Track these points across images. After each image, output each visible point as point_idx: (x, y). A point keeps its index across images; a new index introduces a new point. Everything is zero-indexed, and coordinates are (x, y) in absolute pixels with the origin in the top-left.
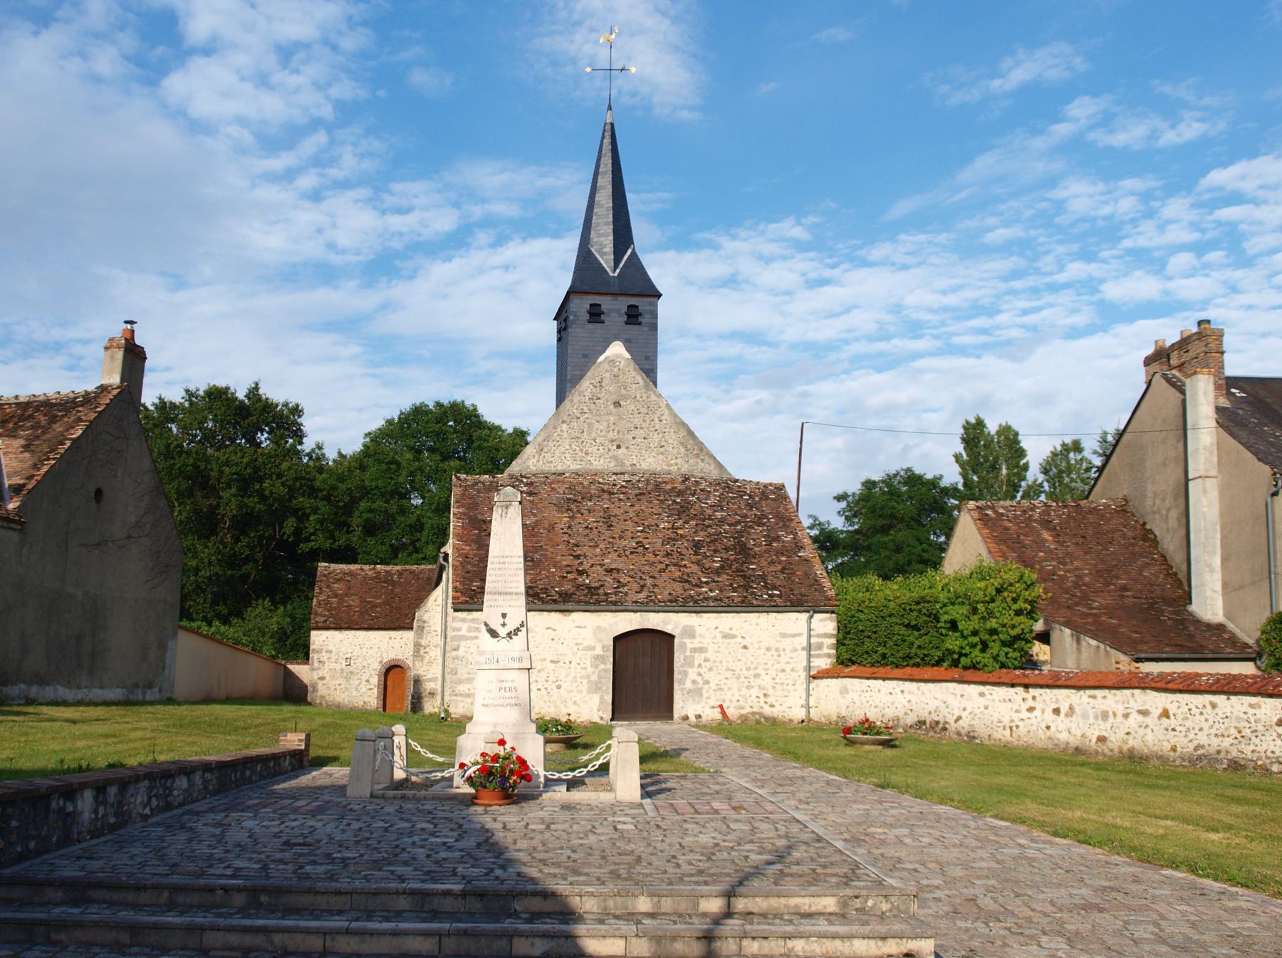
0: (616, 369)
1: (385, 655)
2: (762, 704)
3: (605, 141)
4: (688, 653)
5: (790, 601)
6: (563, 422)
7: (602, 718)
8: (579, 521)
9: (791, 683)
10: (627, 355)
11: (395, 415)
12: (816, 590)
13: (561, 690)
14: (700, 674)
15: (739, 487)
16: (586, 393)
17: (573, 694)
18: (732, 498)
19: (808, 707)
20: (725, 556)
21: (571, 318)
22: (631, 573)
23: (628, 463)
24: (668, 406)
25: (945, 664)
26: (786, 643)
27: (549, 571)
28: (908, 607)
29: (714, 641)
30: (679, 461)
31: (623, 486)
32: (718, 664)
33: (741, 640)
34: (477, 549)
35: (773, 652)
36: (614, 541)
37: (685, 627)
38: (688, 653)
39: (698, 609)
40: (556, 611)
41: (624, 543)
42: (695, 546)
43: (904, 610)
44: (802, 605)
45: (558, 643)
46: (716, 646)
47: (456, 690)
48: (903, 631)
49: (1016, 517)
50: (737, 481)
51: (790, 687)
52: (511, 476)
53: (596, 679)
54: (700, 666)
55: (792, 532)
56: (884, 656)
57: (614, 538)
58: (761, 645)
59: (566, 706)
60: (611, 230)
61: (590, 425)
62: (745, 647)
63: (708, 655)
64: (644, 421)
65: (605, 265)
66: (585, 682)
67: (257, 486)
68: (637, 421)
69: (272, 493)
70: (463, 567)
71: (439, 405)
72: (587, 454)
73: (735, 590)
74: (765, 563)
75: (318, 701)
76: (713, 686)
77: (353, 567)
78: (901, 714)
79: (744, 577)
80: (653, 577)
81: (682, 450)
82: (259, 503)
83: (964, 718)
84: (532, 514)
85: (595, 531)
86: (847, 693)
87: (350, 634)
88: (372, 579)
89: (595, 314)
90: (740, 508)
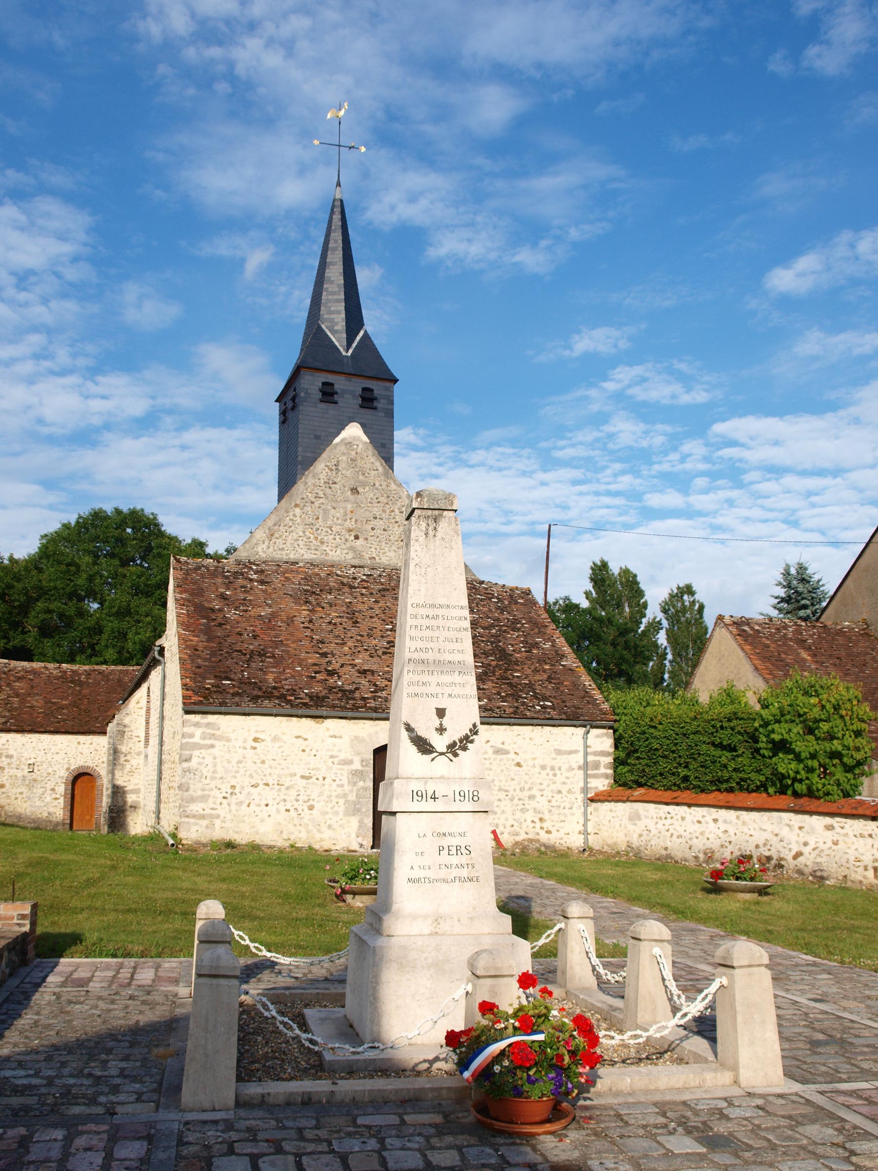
0: (353, 453)
1: (72, 761)
2: (538, 830)
6: (296, 506)
7: (361, 846)
9: (568, 806)
10: (365, 439)
12: (588, 702)
13: (315, 811)
15: (486, 589)
16: (321, 476)
17: (328, 817)
18: (481, 600)
19: (586, 833)
21: (302, 394)
23: (367, 556)
26: (562, 761)
27: (294, 670)
31: (363, 580)
33: (515, 756)
34: (208, 641)
35: (548, 771)
41: (374, 642)
44: (577, 719)
45: (309, 755)
46: (487, 762)
47: (188, 809)
49: (772, 634)
50: (482, 582)
51: (567, 811)
52: (238, 562)
55: (549, 639)
56: (686, 779)
57: (362, 636)
58: (536, 764)
59: (319, 831)
61: (325, 511)
62: (519, 765)
64: (384, 511)
65: (337, 344)
66: (341, 801)
68: (376, 510)
70: (192, 660)
72: (322, 543)
74: (529, 671)
84: (267, 605)
86: (640, 819)
89: (328, 394)
90: (490, 610)
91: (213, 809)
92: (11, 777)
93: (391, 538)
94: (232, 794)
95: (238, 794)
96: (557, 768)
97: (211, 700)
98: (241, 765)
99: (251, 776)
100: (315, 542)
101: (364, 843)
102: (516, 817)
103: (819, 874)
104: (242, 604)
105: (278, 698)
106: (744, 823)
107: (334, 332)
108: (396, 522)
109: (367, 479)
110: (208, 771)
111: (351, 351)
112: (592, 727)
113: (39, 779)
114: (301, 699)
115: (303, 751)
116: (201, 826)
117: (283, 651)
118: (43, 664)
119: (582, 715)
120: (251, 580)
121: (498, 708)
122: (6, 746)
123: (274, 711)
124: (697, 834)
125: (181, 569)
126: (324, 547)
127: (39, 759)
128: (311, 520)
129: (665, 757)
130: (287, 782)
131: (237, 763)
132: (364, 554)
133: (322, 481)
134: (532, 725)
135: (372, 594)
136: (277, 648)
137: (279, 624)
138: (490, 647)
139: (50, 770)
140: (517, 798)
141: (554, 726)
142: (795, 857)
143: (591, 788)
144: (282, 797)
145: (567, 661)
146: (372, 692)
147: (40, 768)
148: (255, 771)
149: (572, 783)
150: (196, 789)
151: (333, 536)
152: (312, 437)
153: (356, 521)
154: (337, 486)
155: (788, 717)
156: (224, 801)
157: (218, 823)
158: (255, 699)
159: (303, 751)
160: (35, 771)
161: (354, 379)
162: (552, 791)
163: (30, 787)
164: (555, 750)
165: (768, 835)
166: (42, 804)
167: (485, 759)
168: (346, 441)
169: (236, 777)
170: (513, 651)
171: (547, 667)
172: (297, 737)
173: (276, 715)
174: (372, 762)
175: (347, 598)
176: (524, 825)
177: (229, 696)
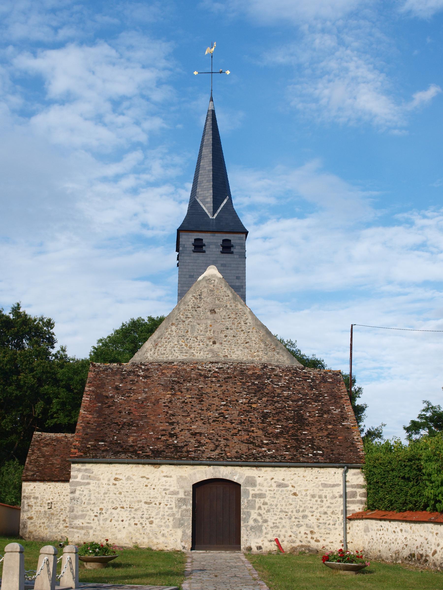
0: (212, 286)
2: (309, 539)
4: (250, 498)
5: (329, 459)
6: (173, 324)
8: (178, 397)
9: (332, 523)
10: (220, 276)
11: (118, 327)
12: (351, 451)
13: (154, 525)
14: (260, 515)
15: (305, 373)
16: (189, 303)
17: (162, 528)
18: (298, 381)
20: (285, 424)
22: (210, 436)
24: (251, 312)
26: (327, 492)
27: (148, 434)
28: (403, 464)
29: (270, 489)
30: (260, 353)
32: (274, 507)
33: (292, 489)
34: (98, 417)
35: (317, 498)
37: (248, 478)
38: (250, 498)
40: (149, 464)
42: (262, 416)
43: (401, 466)
44: (338, 462)
45: (150, 489)
46: (272, 493)
47: (73, 523)
48: (401, 482)
52: (133, 364)
53: (179, 516)
54: (260, 508)
55: (340, 407)
58: (308, 493)
59: (156, 538)
61: (193, 327)
62: (295, 494)
63: (266, 500)
64: (233, 324)
66: (171, 518)
67: (15, 378)
68: (228, 323)
69: (25, 382)
71: (150, 319)
72: (191, 348)
73: (288, 450)
74: (314, 430)
75: (27, 536)
76: (270, 524)
77: (59, 435)
78: (400, 549)
79: (297, 440)
80: (227, 439)
81: (263, 345)
82: (17, 390)
85: (189, 405)
86: (369, 532)
87: (52, 485)
90: (303, 388)
91: (88, 523)
92: (37, 512)
93: (239, 341)
94: (100, 513)
95: (104, 514)
96: (323, 497)
98: (106, 495)
99: (113, 502)
100: (185, 348)
101: (186, 546)
102: (292, 530)
104: (127, 392)
107: (205, 203)
108: (242, 331)
109: (221, 303)
110: (86, 499)
111: (216, 215)
112: (349, 468)
113: (55, 513)
114: (147, 452)
115: (146, 486)
116: (81, 534)
117: (145, 422)
118: (63, 435)
119: (342, 460)
120: (139, 376)
121: (281, 456)
122: (34, 491)
123: (126, 461)
124: (393, 541)
125: (94, 371)
126: (192, 351)
127: (55, 500)
128: (183, 333)
129: (382, 487)
131: (104, 494)
132: (220, 353)
133: (190, 307)
135: (219, 381)
136: (141, 420)
137: (148, 404)
138: (292, 414)
139: (62, 507)
140: (294, 517)
143: (350, 511)
144: (133, 515)
145: (347, 422)
146: (195, 447)
147: (56, 505)
148: (115, 499)
149: (335, 507)
150: (78, 511)
151: (198, 343)
152: (188, 276)
153: (214, 332)
156: (96, 519)
157: (91, 532)
158: (116, 453)
159: (146, 486)
160: (53, 507)
161: (217, 235)
162: (320, 512)
163: (49, 519)
164: (322, 484)
166: (57, 530)
167: (270, 490)
168: (206, 278)
169: (103, 503)
171: (330, 427)
172: (143, 477)
173: (128, 463)
174: (191, 493)
175: (200, 385)
176: (299, 536)
177: (100, 452)
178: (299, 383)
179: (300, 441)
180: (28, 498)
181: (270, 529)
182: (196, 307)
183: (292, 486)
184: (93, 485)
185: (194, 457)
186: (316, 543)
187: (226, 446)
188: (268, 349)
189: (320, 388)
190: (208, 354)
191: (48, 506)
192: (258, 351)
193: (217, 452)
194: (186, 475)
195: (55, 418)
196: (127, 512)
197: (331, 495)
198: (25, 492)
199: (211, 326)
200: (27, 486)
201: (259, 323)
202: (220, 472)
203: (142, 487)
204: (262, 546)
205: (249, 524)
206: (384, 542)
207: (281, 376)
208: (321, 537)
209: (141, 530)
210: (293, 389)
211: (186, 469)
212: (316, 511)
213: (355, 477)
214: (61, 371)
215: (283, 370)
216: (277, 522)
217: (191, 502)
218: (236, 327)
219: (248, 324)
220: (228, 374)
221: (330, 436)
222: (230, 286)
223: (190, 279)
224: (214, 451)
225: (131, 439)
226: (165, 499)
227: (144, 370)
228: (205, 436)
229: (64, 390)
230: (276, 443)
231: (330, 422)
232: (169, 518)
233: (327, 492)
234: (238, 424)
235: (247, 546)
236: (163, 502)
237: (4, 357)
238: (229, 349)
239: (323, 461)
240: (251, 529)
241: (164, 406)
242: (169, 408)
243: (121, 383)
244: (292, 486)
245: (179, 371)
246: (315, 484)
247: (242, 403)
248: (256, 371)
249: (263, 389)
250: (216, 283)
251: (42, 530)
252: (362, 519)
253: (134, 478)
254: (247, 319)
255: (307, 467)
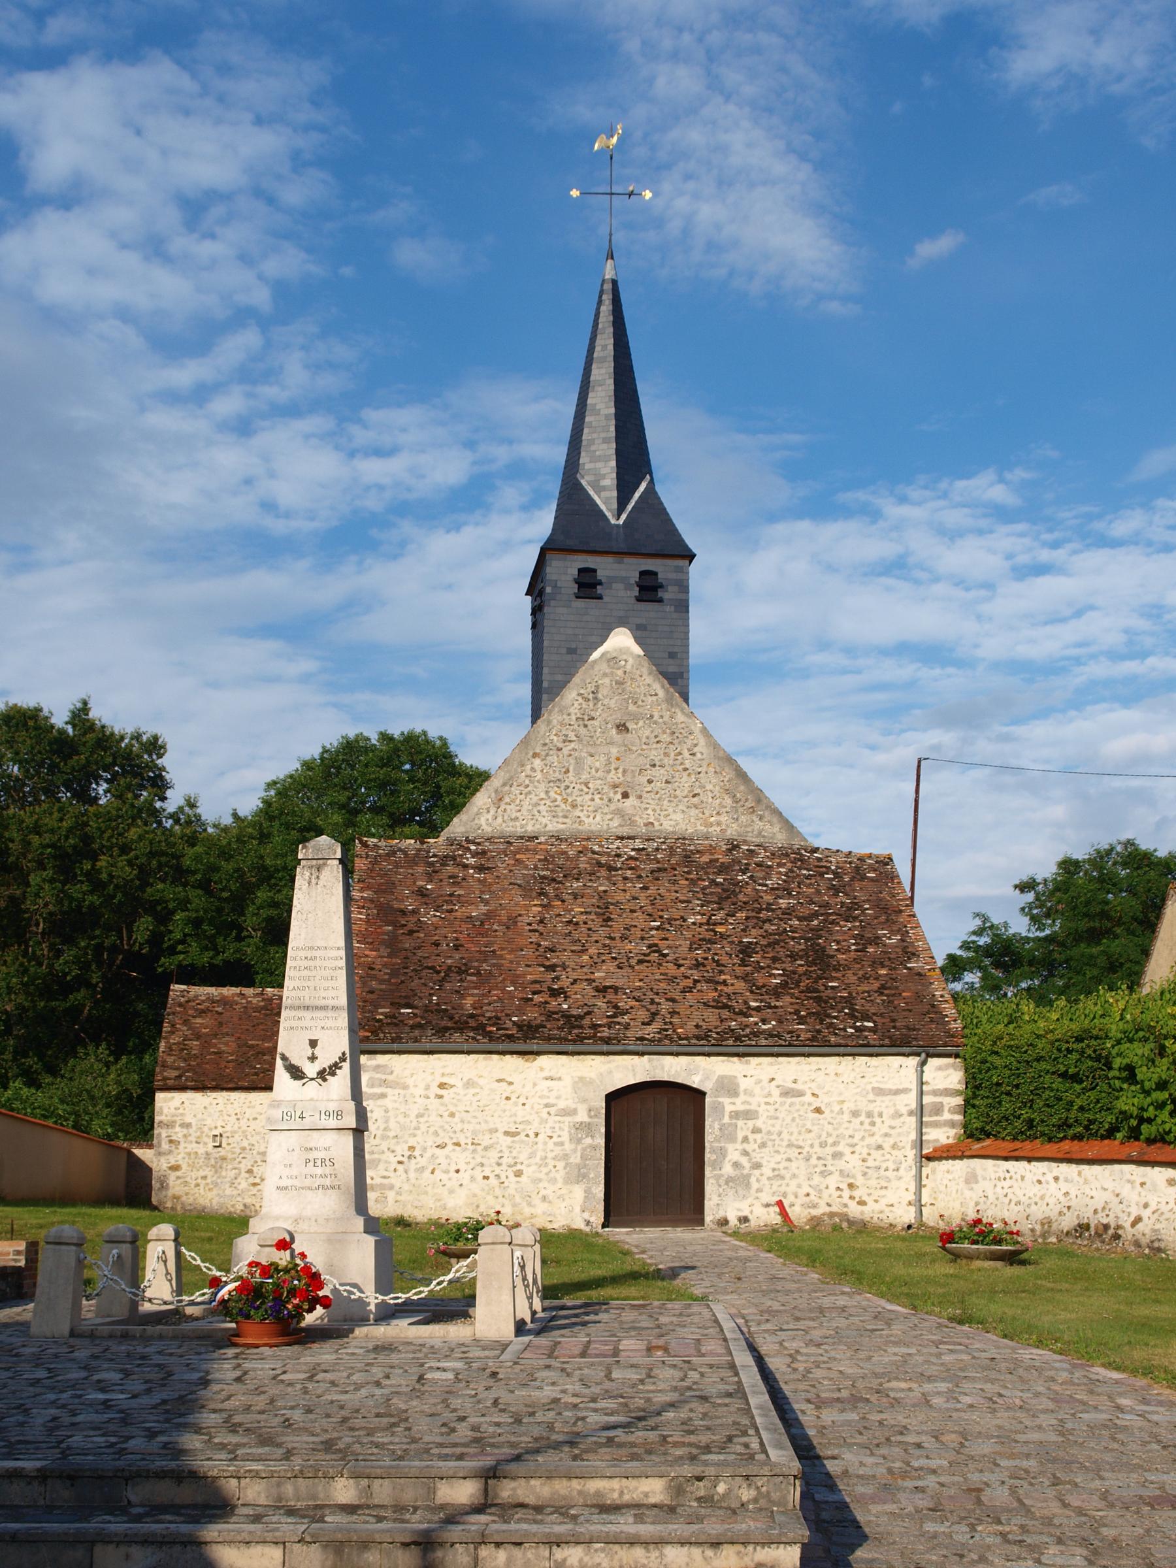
0: (620, 672)
2: (846, 1200)
3: (603, 308)
5: (889, 1037)
6: (535, 755)
7: (588, 1223)
9: (892, 1166)
12: (932, 1021)
13: (524, 1179)
14: (745, 1153)
15: (819, 860)
16: (572, 710)
17: (541, 1185)
18: (807, 877)
19: (919, 1205)
21: (548, 590)
22: (636, 994)
24: (704, 731)
25: (1119, 1135)
26: (884, 1104)
27: (503, 990)
29: (767, 1100)
30: (723, 818)
31: (631, 858)
32: (774, 1137)
33: (812, 1099)
35: (863, 1118)
36: (612, 943)
37: (721, 1079)
38: (726, 1120)
39: (741, 1049)
40: (512, 1053)
41: (629, 947)
42: (741, 952)
43: (1059, 1050)
44: (908, 1044)
45: (516, 1104)
48: (1058, 1083)
50: (816, 850)
51: (889, 1174)
52: (451, 842)
54: (745, 1139)
55: (899, 930)
56: (1030, 1123)
57: (613, 939)
59: (530, 1204)
60: (613, 451)
61: (579, 761)
62: (818, 1110)
63: (759, 1123)
64: (666, 755)
65: (603, 507)
66: (561, 1165)
67: (87, 866)
68: (655, 754)
69: (111, 876)
71: (385, 737)
72: (574, 806)
74: (853, 979)
75: (169, 1205)
76: (767, 1171)
77: (229, 991)
78: (1053, 1215)
79: (818, 1000)
80: (673, 1000)
81: (728, 801)
82: (91, 892)
83: (1145, 1219)
84: (484, 901)
85: (583, 929)
86: (977, 1182)
87: (221, 1097)
88: (258, 1009)
89: (588, 585)
90: (818, 892)
93: (678, 793)
96: (876, 1114)
97: (381, 1036)
99: (436, 1134)
100: (563, 806)
101: (592, 1219)
102: (812, 1183)
103: (1156, 1245)
104: (446, 901)
105: (473, 1029)
106: (1086, 1182)
108: (686, 769)
109: (641, 710)
112: (930, 1055)
114: (507, 1029)
115: (508, 1098)
117: (494, 965)
120: (466, 866)
123: (465, 1047)
126: (577, 813)
128: (557, 774)
130: (486, 1140)
132: (637, 818)
133: (574, 718)
134: (838, 1055)
135: (640, 877)
136: (485, 961)
137: (495, 927)
138: (803, 947)
141: (871, 1055)
142: (1133, 1225)
143: (928, 1141)
144: (479, 1160)
145: (916, 962)
146: (608, 1017)
148: (442, 1127)
149: (899, 1134)
151: (590, 796)
152: (564, 651)
153: (624, 771)
154: (596, 723)
155: (1141, 1034)
158: (441, 1032)
159: (508, 1098)
162: (868, 1146)
164: (873, 1089)
165: (1107, 1196)
167: (767, 1104)
168: (609, 656)
169: (415, 1136)
170: (837, 950)
171: (883, 972)
172: (499, 1081)
173: (469, 1053)
174: (603, 1111)
175: (601, 885)
177: (407, 1029)
178: (808, 881)
179: (826, 1002)
180: (169, 1125)
181: (767, 1182)
182: (586, 718)
183: (813, 1094)
184: (396, 1098)
185: (609, 1038)
186: (860, 1208)
187: (673, 1013)
188: (741, 810)
189: (854, 890)
190: (611, 820)
191: (214, 1141)
192: (718, 813)
193: (655, 1027)
194: (593, 1075)
195: (180, 953)
196: (468, 1154)
197: (892, 1111)
198: (161, 1114)
199: (618, 759)
200: (165, 1100)
201: (721, 754)
202: (663, 1068)
203: (498, 1100)
204: (750, 1217)
205: (723, 1171)
206: (1013, 1203)
207: (770, 867)
208: (869, 1195)
209: (497, 1190)
210: (798, 893)
211: (592, 1063)
212: (862, 1143)
213: (941, 1074)
214: (191, 852)
215: (773, 854)
216: (781, 1166)
217: (603, 1130)
218: (671, 762)
219: (699, 756)
220: (658, 862)
221: (886, 992)
222: (661, 673)
223: (569, 657)
224: (648, 1024)
225: (468, 1002)
226: (548, 1126)
227: (475, 855)
228: (625, 993)
229: (200, 892)
230: (776, 1007)
231: (882, 963)
232: (557, 1163)
233: (884, 1105)
234: (691, 969)
235: (718, 1217)
236: (542, 1131)
237: (61, 820)
238: (658, 808)
239: (877, 1043)
240: (727, 1183)
241: (530, 931)
242: (541, 934)
243: (430, 881)
244: (813, 1094)
245: (553, 857)
246: (859, 1090)
247: (694, 924)
248: (716, 856)
249: (736, 896)
250: (629, 667)
251: (202, 1191)
252: (961, 1158)
253: (481, 1082)
254: (696, 745)
255: (844, 1055)
